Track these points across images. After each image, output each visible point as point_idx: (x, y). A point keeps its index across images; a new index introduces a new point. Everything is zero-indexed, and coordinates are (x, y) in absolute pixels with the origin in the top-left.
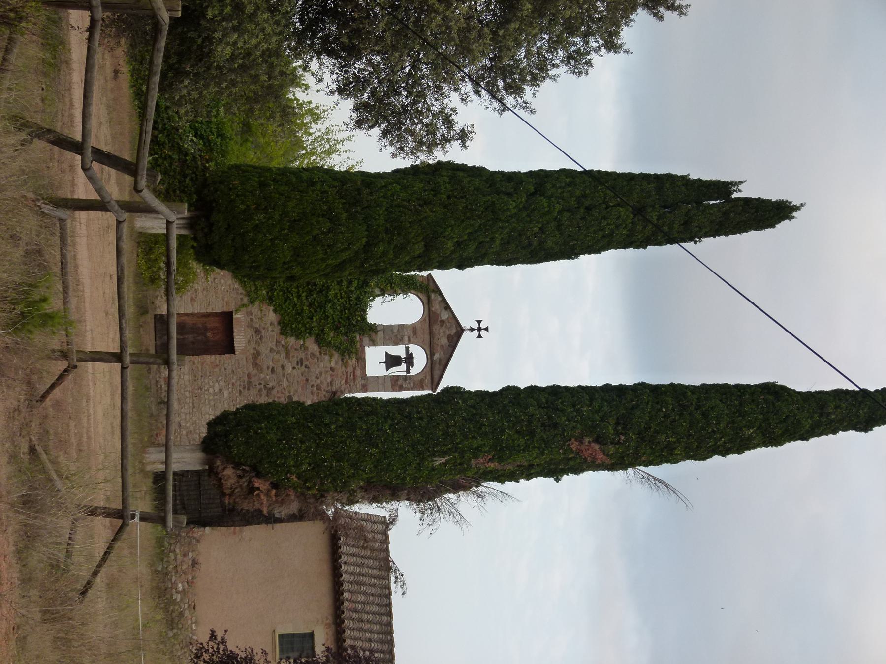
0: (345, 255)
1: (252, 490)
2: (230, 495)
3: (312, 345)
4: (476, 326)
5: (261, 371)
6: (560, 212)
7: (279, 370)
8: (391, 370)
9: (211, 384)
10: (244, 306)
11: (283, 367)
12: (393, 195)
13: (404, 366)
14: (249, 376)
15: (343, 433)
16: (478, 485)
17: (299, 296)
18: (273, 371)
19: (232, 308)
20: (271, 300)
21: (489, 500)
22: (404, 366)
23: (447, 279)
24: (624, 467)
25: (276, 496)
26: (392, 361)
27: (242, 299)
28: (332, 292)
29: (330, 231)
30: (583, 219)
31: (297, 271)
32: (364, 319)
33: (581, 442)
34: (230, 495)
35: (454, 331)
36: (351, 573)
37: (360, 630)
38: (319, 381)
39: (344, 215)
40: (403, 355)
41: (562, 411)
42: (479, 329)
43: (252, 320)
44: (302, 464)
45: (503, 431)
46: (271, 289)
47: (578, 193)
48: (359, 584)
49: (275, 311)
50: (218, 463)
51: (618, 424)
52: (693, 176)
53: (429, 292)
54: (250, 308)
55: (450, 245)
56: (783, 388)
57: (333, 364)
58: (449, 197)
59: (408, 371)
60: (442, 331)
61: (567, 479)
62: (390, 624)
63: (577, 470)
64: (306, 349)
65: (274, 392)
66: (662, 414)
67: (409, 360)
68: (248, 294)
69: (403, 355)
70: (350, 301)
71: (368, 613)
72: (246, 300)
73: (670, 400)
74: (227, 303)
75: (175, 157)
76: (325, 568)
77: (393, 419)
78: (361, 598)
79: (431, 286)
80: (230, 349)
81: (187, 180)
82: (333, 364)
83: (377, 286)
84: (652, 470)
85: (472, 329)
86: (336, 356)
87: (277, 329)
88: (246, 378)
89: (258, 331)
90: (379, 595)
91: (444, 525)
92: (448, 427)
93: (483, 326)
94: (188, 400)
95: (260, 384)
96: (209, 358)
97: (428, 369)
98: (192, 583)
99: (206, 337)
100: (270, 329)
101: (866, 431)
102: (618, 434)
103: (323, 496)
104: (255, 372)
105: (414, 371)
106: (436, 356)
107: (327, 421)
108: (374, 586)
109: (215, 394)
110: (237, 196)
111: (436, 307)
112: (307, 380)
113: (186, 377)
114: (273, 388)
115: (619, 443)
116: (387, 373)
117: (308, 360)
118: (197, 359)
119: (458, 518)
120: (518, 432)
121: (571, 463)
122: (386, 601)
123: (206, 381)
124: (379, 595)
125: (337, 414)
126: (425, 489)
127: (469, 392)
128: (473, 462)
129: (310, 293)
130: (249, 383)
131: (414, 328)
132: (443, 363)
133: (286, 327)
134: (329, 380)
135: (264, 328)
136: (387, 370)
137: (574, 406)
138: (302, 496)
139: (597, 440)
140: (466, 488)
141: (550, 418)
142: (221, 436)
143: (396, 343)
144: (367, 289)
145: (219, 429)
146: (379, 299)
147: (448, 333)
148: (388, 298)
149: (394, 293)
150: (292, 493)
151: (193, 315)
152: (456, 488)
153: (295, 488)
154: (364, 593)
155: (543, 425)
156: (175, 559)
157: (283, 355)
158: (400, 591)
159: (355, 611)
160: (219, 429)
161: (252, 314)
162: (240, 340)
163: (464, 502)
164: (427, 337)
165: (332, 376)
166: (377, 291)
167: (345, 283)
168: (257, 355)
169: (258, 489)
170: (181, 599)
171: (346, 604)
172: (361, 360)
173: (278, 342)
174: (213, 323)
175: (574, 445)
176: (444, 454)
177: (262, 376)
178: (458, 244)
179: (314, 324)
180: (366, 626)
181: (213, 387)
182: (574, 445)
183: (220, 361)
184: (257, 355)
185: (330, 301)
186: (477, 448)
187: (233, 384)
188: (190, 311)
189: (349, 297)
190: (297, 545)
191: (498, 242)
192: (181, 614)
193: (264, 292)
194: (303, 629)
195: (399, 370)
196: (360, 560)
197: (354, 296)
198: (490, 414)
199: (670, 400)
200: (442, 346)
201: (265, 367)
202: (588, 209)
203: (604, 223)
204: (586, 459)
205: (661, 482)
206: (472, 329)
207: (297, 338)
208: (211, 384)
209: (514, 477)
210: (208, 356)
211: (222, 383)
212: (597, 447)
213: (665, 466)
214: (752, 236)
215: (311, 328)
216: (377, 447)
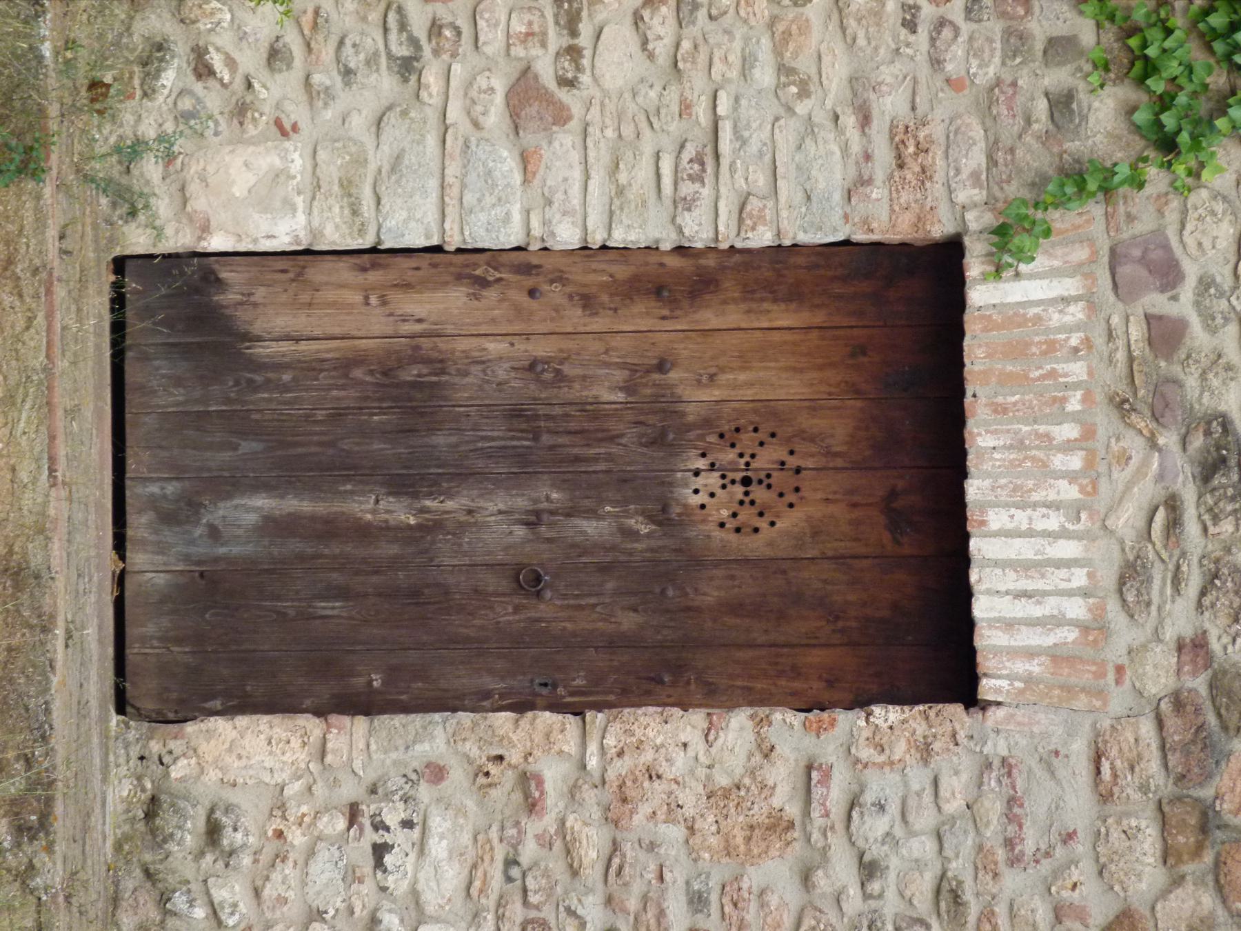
10: (1080, 180)
19: (954, 202)
27: (1061, 104)
43: (1165, 335)
54: (1147, 209)
72: (1105, 114)
74: (908, 147)
80: (924, 646)
96: (688, 748)
99: (663, 515)
151: (523, 266)
174: (752, 366)
183: (811, 773)
188: (498, 224)
210: (688, 725)
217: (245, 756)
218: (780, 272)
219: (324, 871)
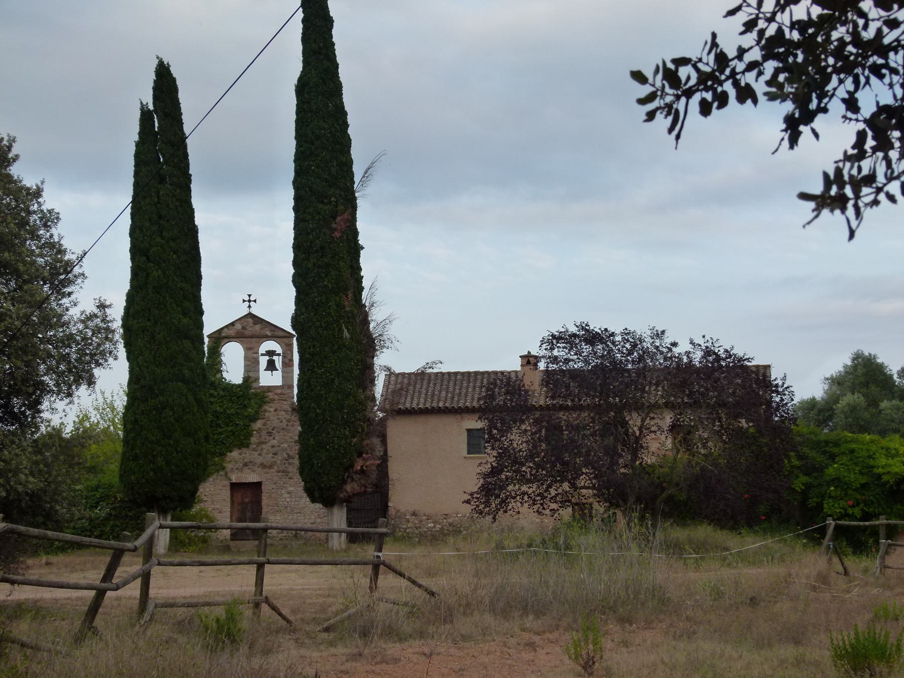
0: (191, 399)
1: (362, 471)
2: (366, 487)
3: (258, 424)
4: (247, 304)
5: (275, 462)
6: (163, 238)
7: (275, 449)
10: (226, 475)
11: (273, 447)
12: (146, 362)
13: (275, 358)
14: (278, 472)
15: (323, 404)
16: (364, 306)
17: (221, 433)
18: (275, 454)
19: (227, 483)
20: (222, 455)
21: (375, 299)
22: (275, 358)
23: (211, 323)
24: (355, 199)
25: (367, 454)
28: (218, 409)
29: (172, 409)
30: (168, 221)
31: (201, 434)
32: (239, 386)
33: (335, 229)
34: (366, 487)
36: (426, 400)
37: (466, 395)
39: (161, 398)
40: (267, 358)
41: (312, 243)
42: (249, 301)
44: (345, 434)
45: (326, 286)
46: (214, 454)
47: (147, 224)
48: (433, 395)
49: (231, 451)
50: (342, 495)
51: (322, 202)
52: (137, 138)
53: (219, 338)
54: (228, 470)
55: (185, 321)
56: (300, 80)
57: (272, 410)
58: (149, 320)
59: (279, 355)
60: (251, 329)
61: (362, 241)
62: (463, 374)
63: (356, 233)
64: (260, 429)
65: (291, 453)
66: (316, 170)
67: (271, 353)
68: (218, 471)
69: (267, 358)
70: (225, 396)
71: (454, 389)
72: (222, 473)
73: (306, 163)
74: (224, 486)
75: (112, 523)
76: (421, 419)
77: (314, 367)
78: (443, 394)
79: (216, 335)
80: (258, 485)
81: (130, 514)
82: (272, 410)
83: (215, 375)
84: (357, 179)
85: (250, 307)
86: (266, 407)
87: (244, 450)
89: (246, 465)
90: (442, 381)
91: (392, 331)
92: (321, 326)
96: (265, 501)
97: (278, 340)
101: (333, 21)
102: (330, 202)
103: (369, 420)
104: (276, 467)
105: (278, 349)
106: (269, 333)
107: (314, 415)
108: (435, 384)
109: (291, 497)
110: (143, 477)
111: (231, 332)
114: (288, 454)
115: (336, 202)
116: (280, 370)
118: (264, 510)
119: (387, 321)
120: (326, 275)
121: (350, 237)
122: (446, 376)
124: (442, 381)
125: (309, 408)
126: (366, 345)
127: (296, 310)
128: (347, 309)
129: (218, 426)
130: (283, 472)
131: (247, 349)
132: (273, 328)
133: (243, 444)
134: (284, 413)
137: (309, 234)
138: (368, 435)
139: (334, 218)
140: (366, 315)
141: (316, 252)
142: (321, 492)
143: (258, 363)
144: (217, 383)
145: (317, 494)
146: (225, 375)
147: (251, 324)
148: (224, 368)
149: (220, 363)
150: (366, 442)
151: (231, 512)
152: (366, 322)
153: (363, 440)
154: (440, 392)
155: (322, 257)
157: (264, 446)
158: (439, 365)
159: (453, 398)
160: (317, 494)
162: (252, 478)
163: (376, 316)
164: (254, 340)
166: (218, 376)
167: (212, 399)
168: (263, 466)
169: (362, 467)
171: (447, 405)
172: (270, 389)
173: (254, 450)
175: (337, 234)
176: (341, 331)
177: (279, 462)
178: (185, 314)
179: (241, 423)
180: (464, 391)
182: (337, 234)
184: (263, 466)
185: (225, 411)
186: (337, 306)
189: (222, 397)
190: (403, 438)
191: (184, 285)
193: (216, 459)
194: (464, 437)
196: (416, 394)
197: (222, 393)
198: (312, 295)
199: (306, 163)
200: (261, 329)
201: (273, 460)
202: (160, 217)
203: (171, 206)
204: (348, 227)
205: (366, 173)
206: (250, 307)
207: (251, 435)
209: (359, 279)
211: (283, 492)
212: (339, 219)
213: (354, 169)
214: (183, 97)
215: (245, 425)
216: (334, 379)
218: (232, 495)
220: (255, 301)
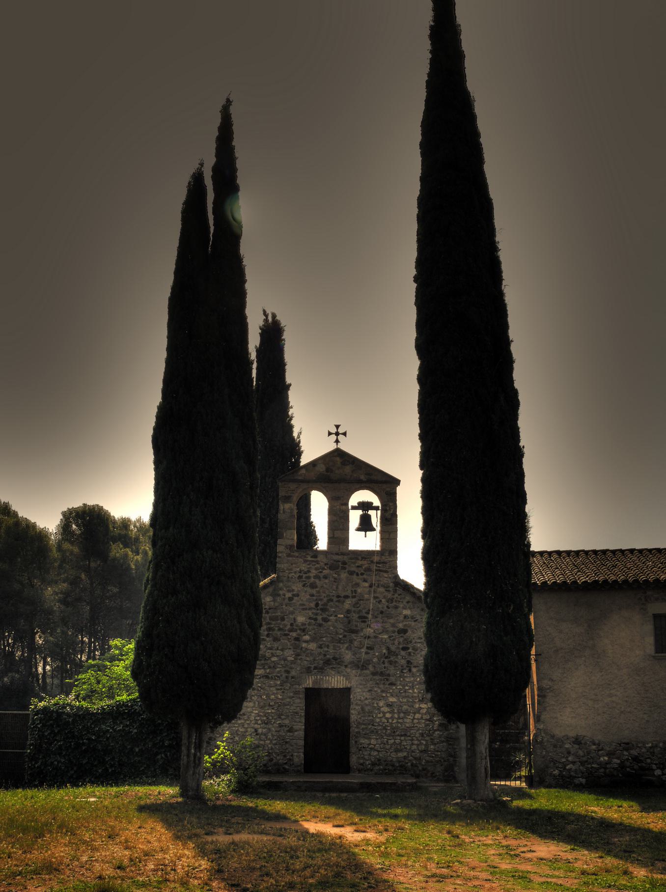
4: (334, 437)
8: (374, 526)
9: (381, 715)
14: (374, 674)
26: (365, 525)
35: (338, 459)
38: (383, 600)
40: (360, 512)
42: (337, 434)
43: (315, 668)
59: (377, 508)
65: (393, 648)
67: (365, 506)
69: (360, 512)
80: (347, 691)
85: (337, 441)
88: (377, 677)
89: (327, 662)
93: (334, 430)
94: (398, 741)
95: (384, 663)
98: (599, 745)
100: (326, 649)
104: (371, 667)
105: (376, 502)
106: (363, 477)
109: (392, 712)
112: (382, 612)
113: (373, 741)
114: (388, 649)
116: (378, 529)
117: (360, 611)
123: (378, 720)
130: (382, 674)
131: (331, 500)
134: (381, 589)
135: (325, 655)
136: (374, 530)
156: (574, 763)
157: (353, 636)
161: (309, 668)
165: (378, 586)
170: (618, 758)
177: (375, 660)
181: (384, 713)
183: (357, 704)
187: (383, 691)
192: (636, 759)
195: (375, 517)
206: (337, 441)
208: (381, 715)
211: (381, 704)
217: (354, 760)
219: (366, 753)
220: (345, 434)
